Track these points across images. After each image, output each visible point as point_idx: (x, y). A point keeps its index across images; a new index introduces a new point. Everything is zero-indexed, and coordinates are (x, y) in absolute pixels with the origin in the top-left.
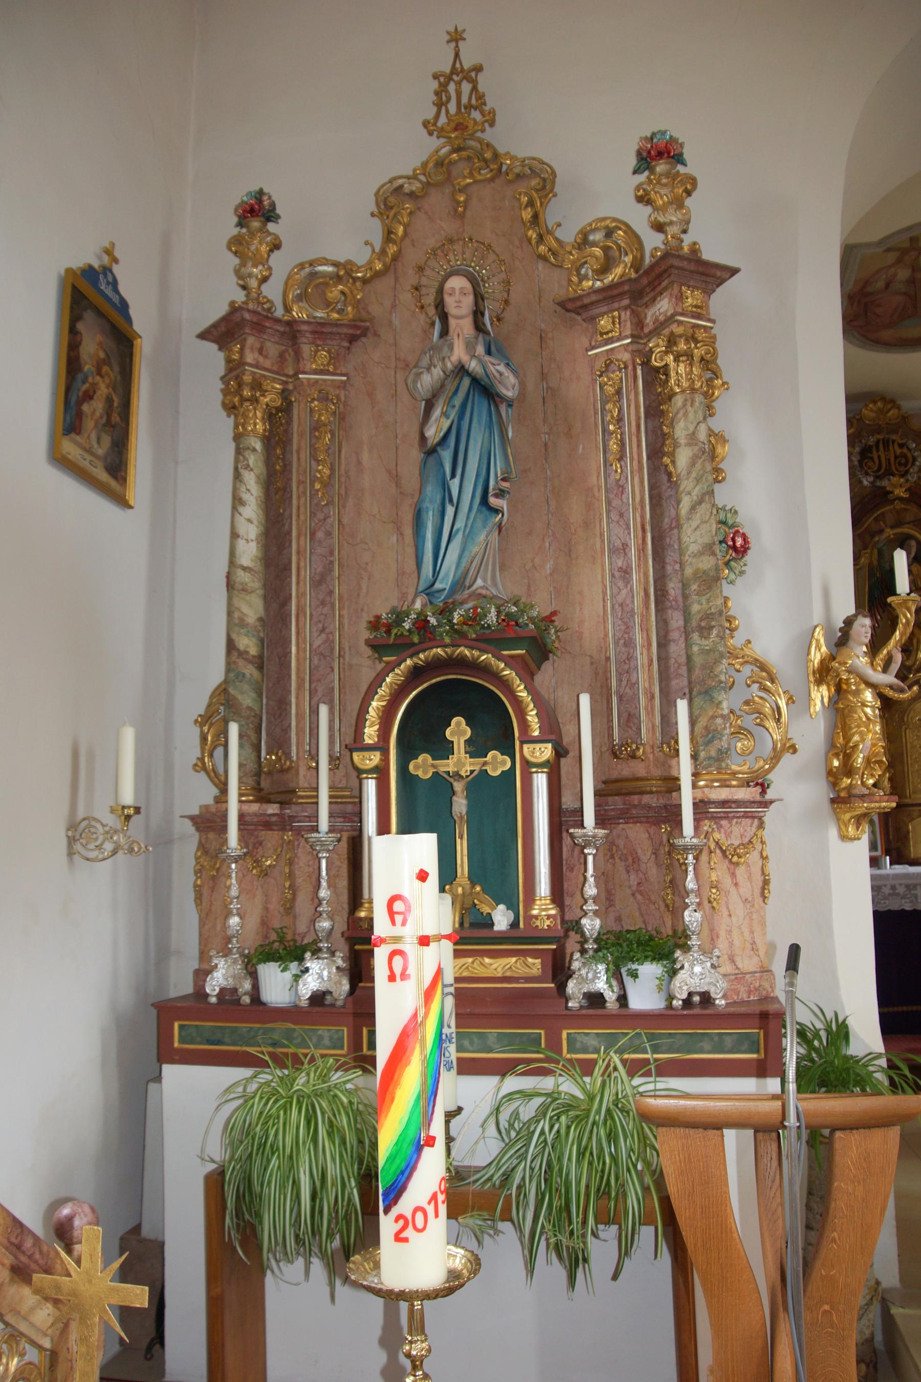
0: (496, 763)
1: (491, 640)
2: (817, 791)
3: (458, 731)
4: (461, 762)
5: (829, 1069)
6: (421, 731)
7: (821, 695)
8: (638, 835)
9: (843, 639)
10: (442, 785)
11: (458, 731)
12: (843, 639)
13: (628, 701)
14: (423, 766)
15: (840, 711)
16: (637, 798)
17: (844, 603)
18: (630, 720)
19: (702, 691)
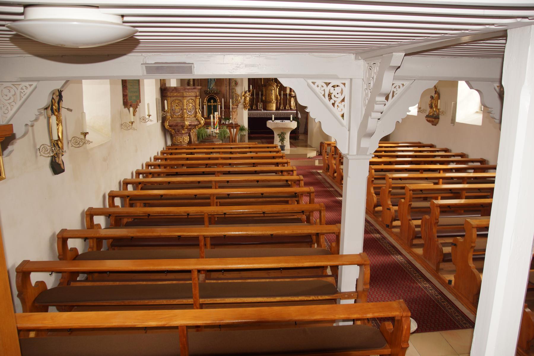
0: (215, 104)
1: (215, 94)
2: (242, 106)
3: (212, 101)
4: (212, 104)
5: (242, 129)
6: (209, 101)
7: (243, 98)
8: (227, 110)
9: (246, 92)
10: (210, 106)
11: (212, 101)
12: (246, 92)
13: (226, 98)
14: (209, 104)
15: (245, 99)
16: (227, 107)
17: (247, 89)
18: (226, 100)
19: (233, 98)
